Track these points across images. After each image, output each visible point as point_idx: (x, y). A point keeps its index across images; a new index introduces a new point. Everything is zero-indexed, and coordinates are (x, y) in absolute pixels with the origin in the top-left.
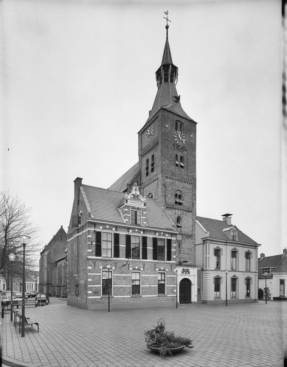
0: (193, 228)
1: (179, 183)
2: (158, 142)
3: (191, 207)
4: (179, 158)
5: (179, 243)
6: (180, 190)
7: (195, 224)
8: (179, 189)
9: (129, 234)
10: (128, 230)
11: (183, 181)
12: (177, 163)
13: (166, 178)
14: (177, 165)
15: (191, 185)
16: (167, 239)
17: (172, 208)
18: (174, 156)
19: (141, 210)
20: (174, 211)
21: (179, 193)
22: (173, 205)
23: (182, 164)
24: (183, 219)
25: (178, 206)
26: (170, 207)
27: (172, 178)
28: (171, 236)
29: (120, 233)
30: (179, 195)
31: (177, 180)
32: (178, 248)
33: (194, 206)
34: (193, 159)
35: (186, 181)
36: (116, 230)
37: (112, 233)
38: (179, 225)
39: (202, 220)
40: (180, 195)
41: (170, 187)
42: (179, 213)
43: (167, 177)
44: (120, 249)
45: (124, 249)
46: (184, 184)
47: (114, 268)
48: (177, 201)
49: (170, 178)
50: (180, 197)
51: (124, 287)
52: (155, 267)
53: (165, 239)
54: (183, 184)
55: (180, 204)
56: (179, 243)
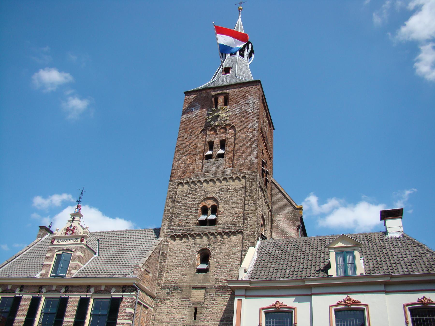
1: (211, 184)
5: (196, 309)
8: (210, 195)
20: (191, 240)
21: (209, 204)
27: (193, 182)
30: (209, 206)
35: (228, 177)
42: (204, 242)
46: (224, 182)
50: (214, 210)
56: (196, 309)
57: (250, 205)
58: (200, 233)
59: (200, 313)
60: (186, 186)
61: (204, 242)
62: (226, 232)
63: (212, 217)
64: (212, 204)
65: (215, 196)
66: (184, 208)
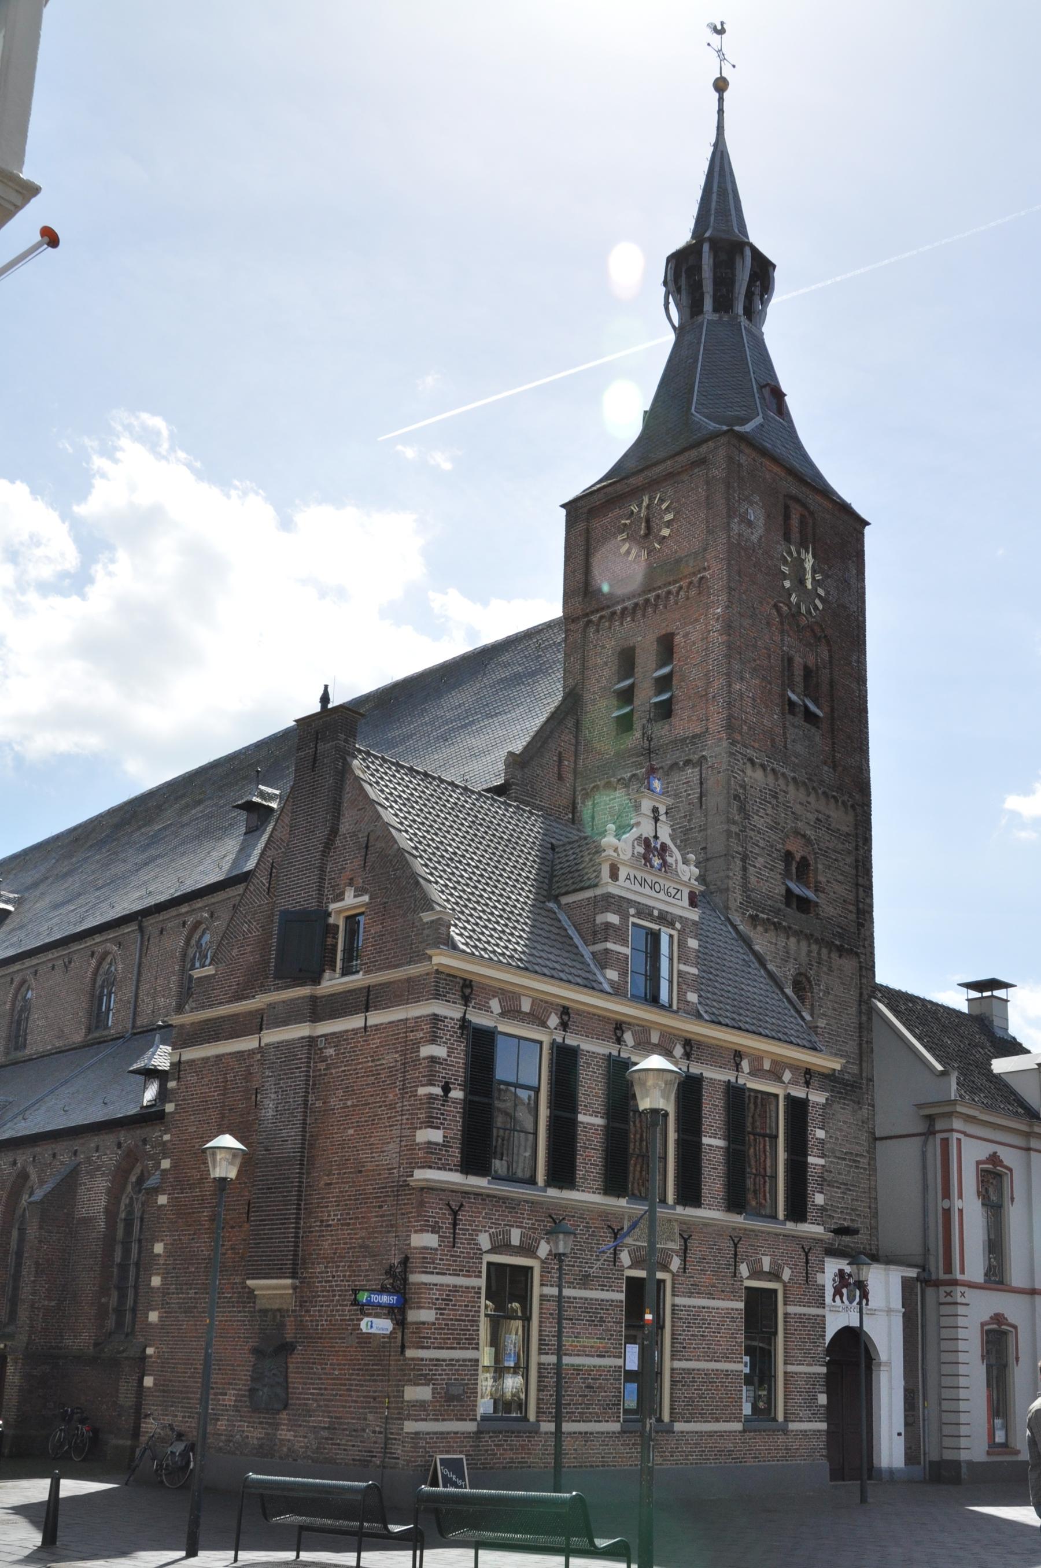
0: (865, 1046)
2: (702, 578)
3: (853, 929)
6: (804, 836)
7: (870, 1019)
9: (623, 1055)
11: (820, 791)
14: (791, 704)
16: (788, 1097)
17: (774, 924)
19: (678, 926)
20: (782, 941)
22: (777, 912)
25: (793, 917)
26: (765, 916)
27: (773, 770)
28: (807, 1084)
29: (584, 1046)
30: (798, 857)
31: (794, 779)
33: (863, 925)
34: (854, 686)
36: (564, 1026)
37: (541, 1043)
39: (899, 1000)
40: (803, 858)
41: (762, 812)
43: (751, 760)
45: (720, 1157)
48: (796, 888)
51: (590, 1369)
52: (736, 1255)
53: (776, 1096)
55: (804, 905)
60: (759, 774)
64: (802, 853)
65: (808, 832)
66: (762, 844)
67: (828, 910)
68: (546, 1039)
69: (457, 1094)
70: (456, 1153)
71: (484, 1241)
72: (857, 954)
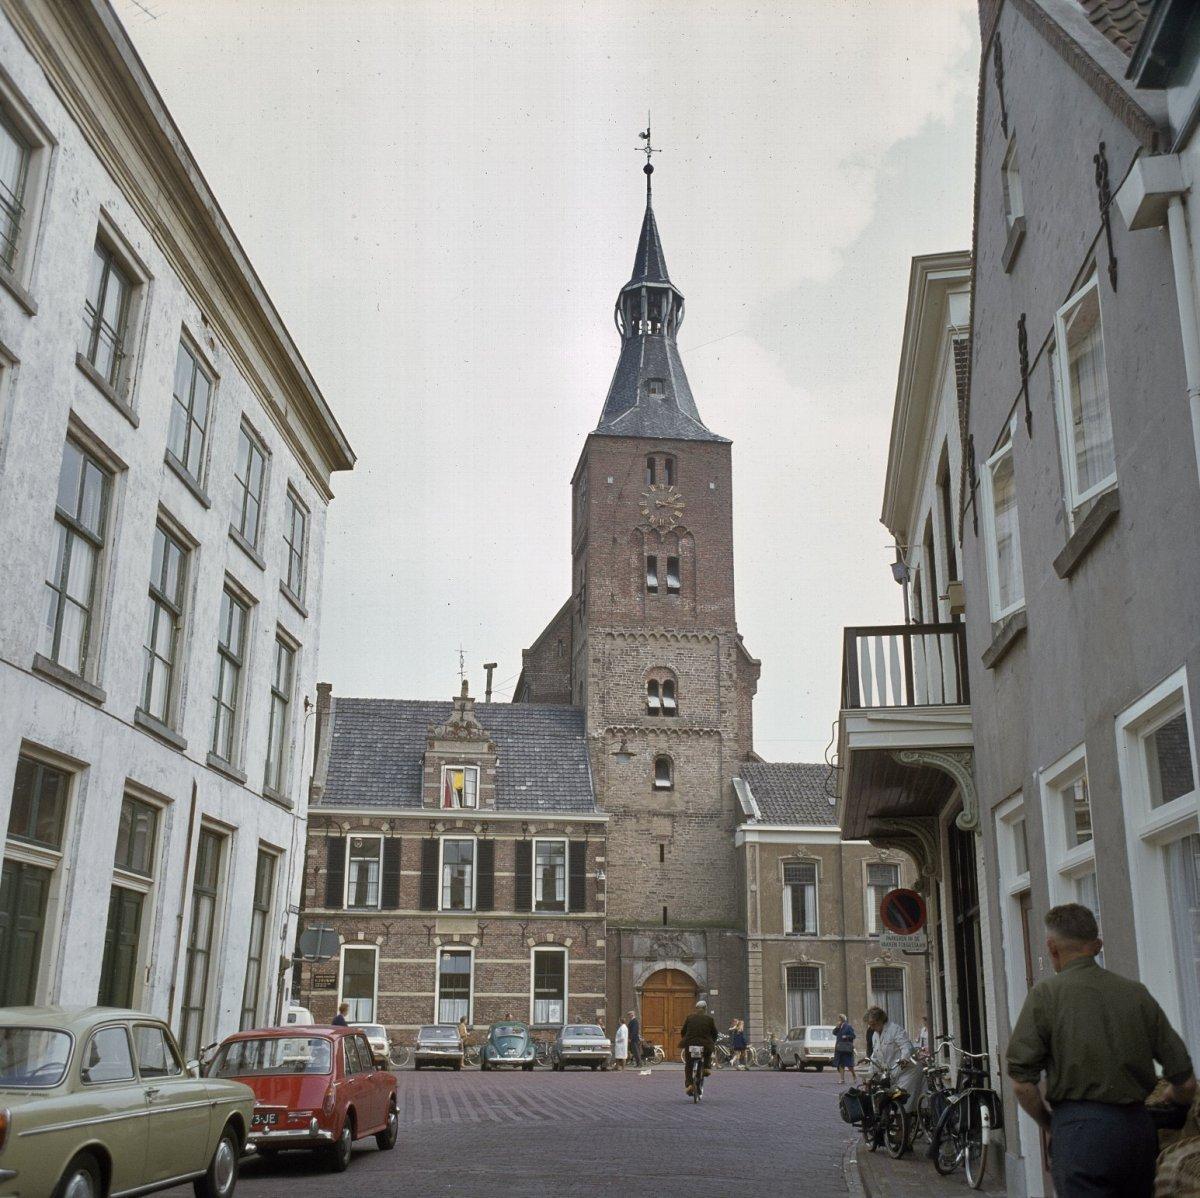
4: (662, 566)
5: (662, 846)
8: (661, 663)
10: (433, 825)
11: (679, 637)
12: (652, 581)
13: (609, 639)
14: (653, 589)
15: (714, 642)
18: (634, 561)
21: (661, 678)
23: (672, 582)
24: (679, 763)
28: (587, 832)
29: (403, 836)
30: (661, 682)
32: (657, 864)
35: (689, 634)
36: (392, 828)
38: (659, 783)
42: (662, 744)
44: (403, 882)
46: (683, 643)
47: (380, 940)
49: (622, 635)
54: (680, 645)
55: (669, 712)
56: (662, 846)
57: (728, 688)
58: (654, 728)
59: (670, 852)
60: (619, 641)
61: (662, 744)
62: (696, 731)
63: (669, 703)
65: (669, 665)
67: (684, 712)
68: (381, 836)
69: (323, 871)
70: (321, 900)
71: (342, 939)
72: (718, 732)
